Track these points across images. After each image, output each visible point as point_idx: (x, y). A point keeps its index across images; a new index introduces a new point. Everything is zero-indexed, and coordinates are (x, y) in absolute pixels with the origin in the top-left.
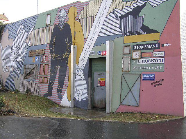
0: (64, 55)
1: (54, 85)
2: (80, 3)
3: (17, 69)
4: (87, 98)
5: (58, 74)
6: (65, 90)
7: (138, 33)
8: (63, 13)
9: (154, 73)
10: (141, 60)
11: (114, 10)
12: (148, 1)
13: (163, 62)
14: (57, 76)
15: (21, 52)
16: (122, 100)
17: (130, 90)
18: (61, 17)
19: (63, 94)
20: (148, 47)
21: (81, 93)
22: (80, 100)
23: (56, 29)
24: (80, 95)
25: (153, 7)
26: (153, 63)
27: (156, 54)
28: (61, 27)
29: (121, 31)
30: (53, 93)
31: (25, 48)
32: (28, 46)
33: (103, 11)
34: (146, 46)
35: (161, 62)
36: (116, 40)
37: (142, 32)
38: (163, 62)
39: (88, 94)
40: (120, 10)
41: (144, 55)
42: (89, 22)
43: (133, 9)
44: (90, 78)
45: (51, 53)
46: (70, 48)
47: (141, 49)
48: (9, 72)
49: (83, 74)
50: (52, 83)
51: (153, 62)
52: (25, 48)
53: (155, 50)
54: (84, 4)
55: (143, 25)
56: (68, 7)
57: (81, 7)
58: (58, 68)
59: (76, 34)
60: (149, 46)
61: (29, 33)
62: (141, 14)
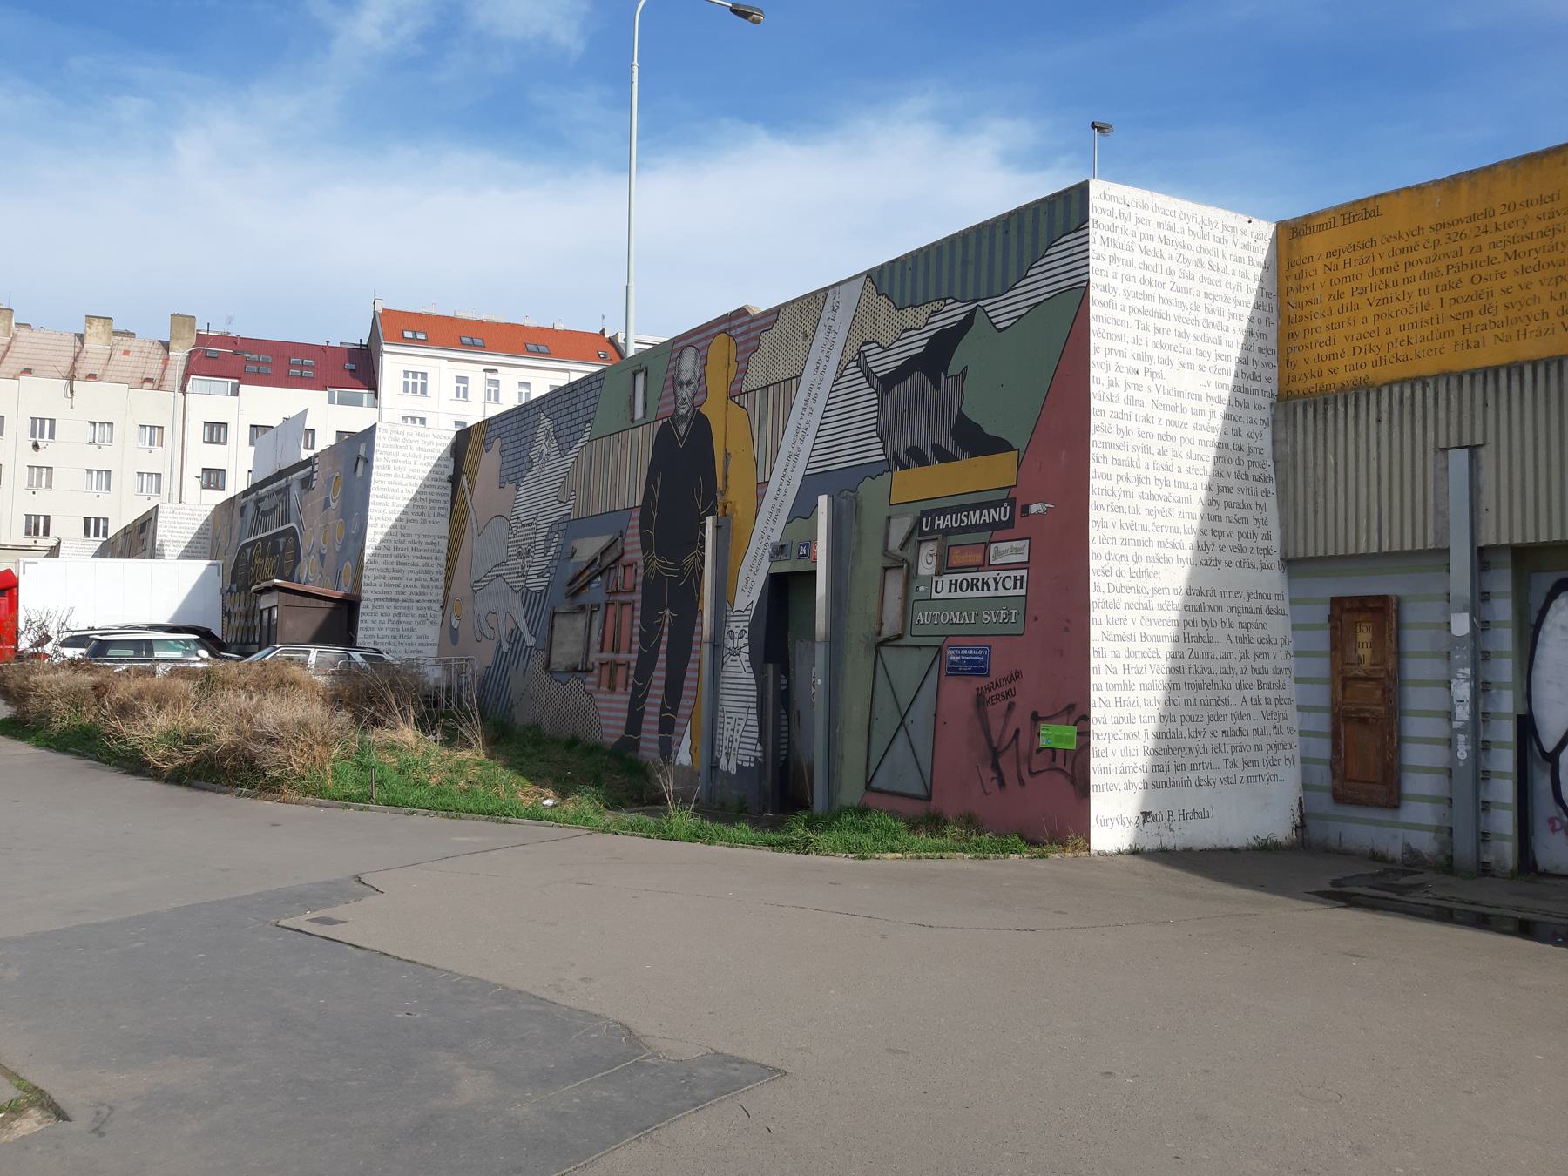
0: (689, 560)
1: (648, 700)
2: (747, 319)
3: (524, 630)
4: (756, 758)
5: (663, 647)
6: (684, 721)
7: (944, 456)
8: (688, 364)
9: (988, 640)
10: (946, 578)
11: (863, 348)
12: (981, 303)
13: (1021, 587)
14: (662, 656)
15: (540, 548)
16: (872, 772)
17: (903, 718)
18: (681, 384)
19: (678, 739)
20: (974, 518)
21: (737, 736)
22: (733, 769)
23: (665, 438)
24: (735, 745)
25: (1000, 330)
26: (986, 593)
27: (1000, 553)
28: (682, 428)
29: (881, 445)
30: (643, 735)
31: (555, 528)
32: (566, 518)
33: (823, 356)
34: (967, 516)
35: (1015, 588)
36: (867, 488)
37: (955, 450)
38: (1021, 587)
39: (761, 740)
40: (885, 349)
41: (957, 558)
42: (776, 406)
43: (925, 342)
44: (770, 666)
45: (644, 549)
46: (703, 526)
47: (948, 532)
48: (497, 638)
49: (747, 649)
50: (641, 688)
51: (989, 589)
52: (555, 528)
53: (998, 534)
54: (762, 322)
55: (961, 417)
56: (707, 338)
57: (753, 334)
58: (667, 621)
59: (731, 462)
60: (978, 512)
61: (571, 455)
62: (954, 367)
